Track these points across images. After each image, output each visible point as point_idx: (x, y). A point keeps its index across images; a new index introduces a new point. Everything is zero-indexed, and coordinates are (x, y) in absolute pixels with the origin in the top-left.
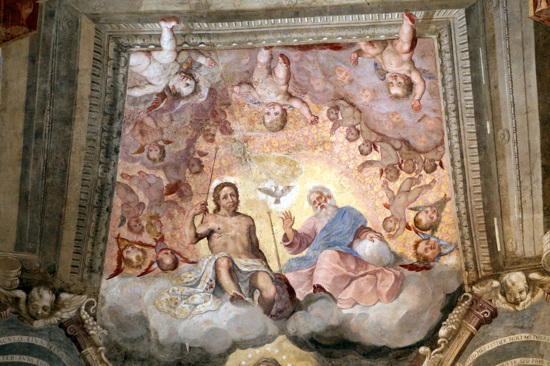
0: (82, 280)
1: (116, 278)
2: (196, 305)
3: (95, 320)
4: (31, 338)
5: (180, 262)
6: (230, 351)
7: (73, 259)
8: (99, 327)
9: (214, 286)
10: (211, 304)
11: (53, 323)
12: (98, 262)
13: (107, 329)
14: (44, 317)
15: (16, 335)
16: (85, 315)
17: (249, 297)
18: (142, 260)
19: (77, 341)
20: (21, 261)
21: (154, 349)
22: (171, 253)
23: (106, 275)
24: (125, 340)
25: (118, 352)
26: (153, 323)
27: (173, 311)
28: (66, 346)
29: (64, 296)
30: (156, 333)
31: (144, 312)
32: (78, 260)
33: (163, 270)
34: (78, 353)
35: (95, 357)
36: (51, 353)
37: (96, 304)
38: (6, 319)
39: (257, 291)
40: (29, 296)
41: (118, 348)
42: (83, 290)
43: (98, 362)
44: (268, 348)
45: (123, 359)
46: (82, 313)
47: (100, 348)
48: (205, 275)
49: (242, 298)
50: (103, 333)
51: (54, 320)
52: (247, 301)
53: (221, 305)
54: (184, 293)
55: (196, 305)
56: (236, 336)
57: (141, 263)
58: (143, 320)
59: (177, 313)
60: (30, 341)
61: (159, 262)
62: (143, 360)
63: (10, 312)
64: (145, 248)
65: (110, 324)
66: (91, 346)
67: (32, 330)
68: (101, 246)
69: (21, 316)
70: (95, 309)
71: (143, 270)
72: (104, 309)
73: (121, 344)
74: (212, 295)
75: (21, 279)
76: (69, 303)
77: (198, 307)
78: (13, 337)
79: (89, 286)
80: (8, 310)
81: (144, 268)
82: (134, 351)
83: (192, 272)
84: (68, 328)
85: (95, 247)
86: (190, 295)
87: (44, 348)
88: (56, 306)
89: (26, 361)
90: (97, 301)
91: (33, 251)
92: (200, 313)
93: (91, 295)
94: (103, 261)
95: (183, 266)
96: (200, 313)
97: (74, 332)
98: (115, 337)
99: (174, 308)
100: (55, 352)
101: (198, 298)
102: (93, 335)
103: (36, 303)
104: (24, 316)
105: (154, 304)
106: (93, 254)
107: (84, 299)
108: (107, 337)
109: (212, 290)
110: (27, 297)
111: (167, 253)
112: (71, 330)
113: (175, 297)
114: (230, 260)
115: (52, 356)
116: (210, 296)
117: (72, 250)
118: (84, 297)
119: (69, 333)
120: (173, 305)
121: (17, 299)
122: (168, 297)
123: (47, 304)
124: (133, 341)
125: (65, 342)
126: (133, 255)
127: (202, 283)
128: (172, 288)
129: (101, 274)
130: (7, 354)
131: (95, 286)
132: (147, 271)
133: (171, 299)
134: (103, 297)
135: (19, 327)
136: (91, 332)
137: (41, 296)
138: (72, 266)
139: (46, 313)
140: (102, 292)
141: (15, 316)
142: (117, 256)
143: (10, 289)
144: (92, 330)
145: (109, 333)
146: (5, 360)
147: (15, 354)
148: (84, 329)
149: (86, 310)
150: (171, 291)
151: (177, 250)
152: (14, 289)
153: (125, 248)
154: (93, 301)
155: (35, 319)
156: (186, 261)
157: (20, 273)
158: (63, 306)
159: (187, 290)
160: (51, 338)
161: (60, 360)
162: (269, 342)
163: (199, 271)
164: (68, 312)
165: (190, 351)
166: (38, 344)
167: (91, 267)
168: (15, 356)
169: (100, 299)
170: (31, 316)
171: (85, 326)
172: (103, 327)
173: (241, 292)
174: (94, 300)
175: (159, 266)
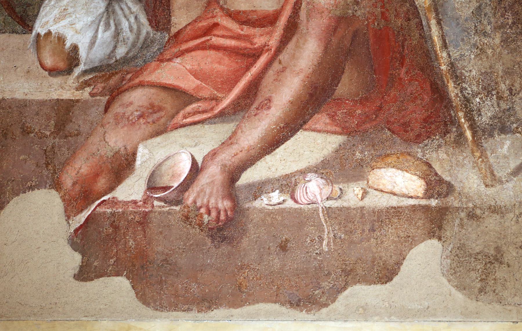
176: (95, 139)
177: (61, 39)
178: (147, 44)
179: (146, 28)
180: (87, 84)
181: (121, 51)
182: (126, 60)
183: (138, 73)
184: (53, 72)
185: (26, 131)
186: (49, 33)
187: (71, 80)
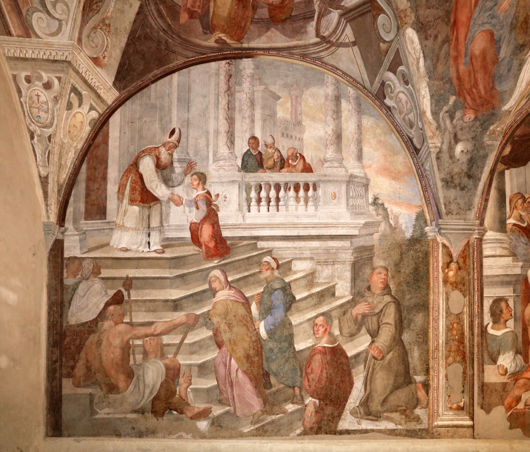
176: (512, 392)
177: (503, 366)
178: (524, 367)
179: (523, 363)
180: (510, 378)
181: (517, 369)
182: (518, 372)
183: (522, 375)
184: (502, 375)
185: (496, 391)
186: (501, 365)
187: (506, 377)
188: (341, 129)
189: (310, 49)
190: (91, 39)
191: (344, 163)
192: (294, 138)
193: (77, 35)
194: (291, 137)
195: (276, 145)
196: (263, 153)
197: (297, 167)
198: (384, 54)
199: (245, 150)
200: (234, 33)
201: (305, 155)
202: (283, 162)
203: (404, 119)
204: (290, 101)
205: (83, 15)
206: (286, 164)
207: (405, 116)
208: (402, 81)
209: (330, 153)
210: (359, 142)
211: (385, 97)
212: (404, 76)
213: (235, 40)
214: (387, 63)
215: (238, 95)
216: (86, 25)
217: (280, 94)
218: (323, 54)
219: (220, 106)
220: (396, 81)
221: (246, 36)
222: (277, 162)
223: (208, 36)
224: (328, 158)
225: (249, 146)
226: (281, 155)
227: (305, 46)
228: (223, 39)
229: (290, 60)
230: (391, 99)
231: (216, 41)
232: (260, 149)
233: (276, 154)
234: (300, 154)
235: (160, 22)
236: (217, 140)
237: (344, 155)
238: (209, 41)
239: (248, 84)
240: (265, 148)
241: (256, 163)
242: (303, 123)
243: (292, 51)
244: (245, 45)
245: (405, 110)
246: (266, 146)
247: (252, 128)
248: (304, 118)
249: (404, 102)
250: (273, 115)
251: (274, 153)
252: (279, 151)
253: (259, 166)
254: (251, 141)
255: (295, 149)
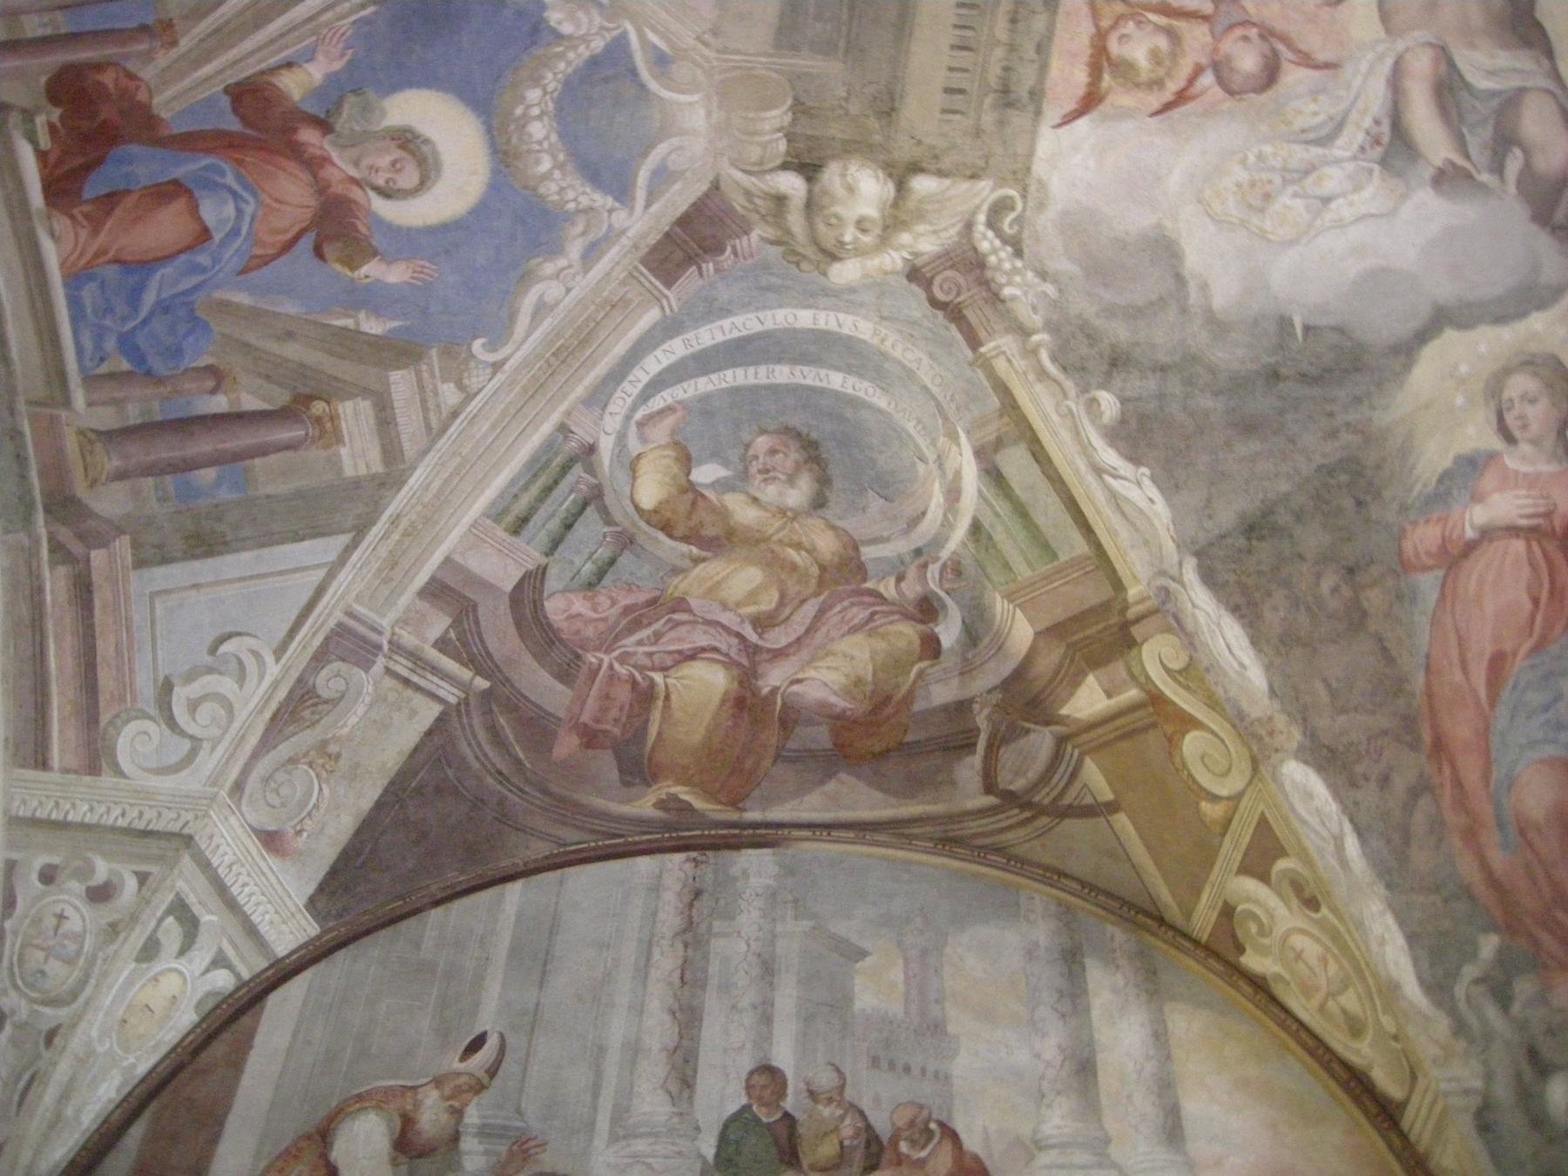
0: (978, 133)
1: (1082, 124)
2: (1326, 201)
3: (1018, 253)
4: (822, 316)
5: (1286, 66)
6: (1423, 336)
7: (951, 69)
8: (1030, 275)
9: (1386, 139)
10: (1372, 194)
11: (889, 268)
12: (1026, 77)
13: (1055, 282)
14: (860, 252)
15: (780, 306)
16: (986, 241)
17: (1491, 171)
18: (1167, 63)
19: (964, 316)
20: (795, 78)
21: (1198, 337)
22: (1262, 36)
23: (1052, 114)
24: (1110, 312)
25: (1091, 346)
26: (1193, 261)
27: (1255, 220)
28: (930, 335)
29: (923, 185)
30: (1204, 287)
31: (1168, 224)
32: (966, 70)
33: (1231, 93)
34: (969, 354)
35: (1020, 364)
36: (884, 355)
37: (1019, 206)
38: (750, 262)
39: (1517, 151)
40: (817, 189)
41: (1092, 337)
42: (981, 163)
43: (1031, 377)
44: (1537, 322)
45: (1105, 367)
46: (977, 235)
47: (1036, 338)
48: (1360, 105)
49: (1469, 176)
50: (1045, 294)
51: (893, 260)
52: (1483, 187)
53: (1404, 197)
54: (1293, 164)
55: (1326, 201)
56: (1444, 289)
57: (1161, 72)
58: (1164, 249)
59: (1268, 225)
60: (822, 325)
61: (1220, 68)
62: (1165, 369)
63: (762, 239)
64: (1180, 24)
65: (1062, 265)
66: (1008, 331)
67: (827, 292)
68: (1039, 23)
69: (794, 253)
70: (1019, 220)
71: (1168, 94)
72: (1045, 222)
73: (1097, 323)
74: (1377, 168)
75: (790, 138)
76: (937, 206)
77: (1333, 205)
78: (769, 313)
79: (999, 150)
80: (754, 235)
81: (1172, 87)
82: (1137, 344)
83: (1321, 98)
84: (937, 281)
85: (1021, 26)
86: (1309, 169)
87: (864, 342)
88: (896, 218)
89: (809, 382)
90: (1024, 197)
91: (825, 48)
92: (1340, 224)
93: (1003, 179)
94: (1044, 68)
95: (1294, 77)
96: (1340, 224)
97: (954, 293)
98: (1082, 305)
99: (1262, 211)
100: (897, 353)
101: (1333, 179)
102: (1014, 298)
103: (837, 209)
104: (800, 250)
105: (1199, 201)
106: (1012, 48)
107: (985, 191)
108: (1054, 304)
109: (1379, 150)
110: (810, 192)
111: (1246, 39)
112: (945, 287)
113: (1265, 176)
114: (1443, 53)
115: (886, 365)
116: (1370, 172)
117: (948, 37)
118: (984, 185)
119: (940, 296)
120: (1257, 202)
121: (780, 200)
122: (1241, 175)
123: (871, 211)
124: (1134, 313)
125: (926, 323)
126: (1137, 47)
127: (1349, 129)
128: (1255, 150)
129: (1038, 113)
130: (756, 363)
131: (1020, 150)
132: (1181, 97)
133: (1253, 185)
134: (1042, 185)
135: (790, 283)
136: (1007, 292)
137: (851, 189)
138: (949, 91)
139: (867, 239)
140: (1039, 168)
141: (774, 252)
142: (1089, 51)
143: (759, 170)
144: (1009, 283)
145: (1061, 291)
146: (752, 381)
147: (779, 361)
148: (985, 283)
149: (992, 224)
150: (1252, 158)
151: (1279, 26)
152: (772, 170)
153: (1113, 27)
154: (1011, 198)
155: (834, 258)
156: (1307, 60)
157: (788, 118)
158: (920, 216)
159: (1301, 154)
160: (886, 314)
161: (910, 374)
162: (1542, 305)
163: (1343, 93)
164: (935, 232)
165: (1305, 340)
166: (846, 331)
167: (1005, 91)
168: (778, 368)
169: (1032, 189)
170: (824, 251)
171: (989, 274)
172: (1043, 275)
173: (1467, 156)
174: (1012, 192)
175: (1221, 81)
188: (1091, 1044)
189: (966, 824)
190: (273, 785)
191: (1114, 1151)
192: (916, 1071)
193: (234, 774)
194: (907, 1069)
195: (849, 1094)
196: (797, 1114)
197: (929, 1167)
198: (1218, 829)
199: (732, 1108)
200: (718, 785)
201: (959, 1126)
202: (874, 1149)
203: (1322, 1008)
204: (900, 962)
205: (267, 730)
206: (888, 1156)
207: (1326, 1000)
208: (1295, 902)
209: (1057, 1120)
210: (1166, 1089)
211: (1241, 949)
212: (1297, 886)
213: (720, 803)
214: (1232, 849)
215: (717, 945)
216: (268, 751)
217: (866, 944)
218: (1009, 836)
219: (654, 974)
220: (1273, 901)
221: (756, 793)
222: (854, 1148)
223: (634, 790)
224: (1050, 1137)
225: (749, 1095)
226: (869, 1127)
227: (951, 818)
228: (681, 801)
229: (900, 854)
230: (1264, 951)
231: (661, 805)
232: (789, 1104)
233: (848, 1121)
234: (942, 1125)
235: (491, 754)
236: (631, 1073)
237: (1111, 1124)
238: (637, 804)
239: (755, 914)
240: (808, 1102)
241: (774, 1150)
242: (951, 1029)
243: (907, 831)
244: (753, 815)
245: (1323, 982)
246: (812, 1095)
247: (764, 1037)
248: (952, 1012)
249: (1313, 962)
250: (840, 1004)
251: (842, 1118)
252: (861, 1113)
253: (782, 1161)
254: (759, 1080)
255: (921, 1107)
